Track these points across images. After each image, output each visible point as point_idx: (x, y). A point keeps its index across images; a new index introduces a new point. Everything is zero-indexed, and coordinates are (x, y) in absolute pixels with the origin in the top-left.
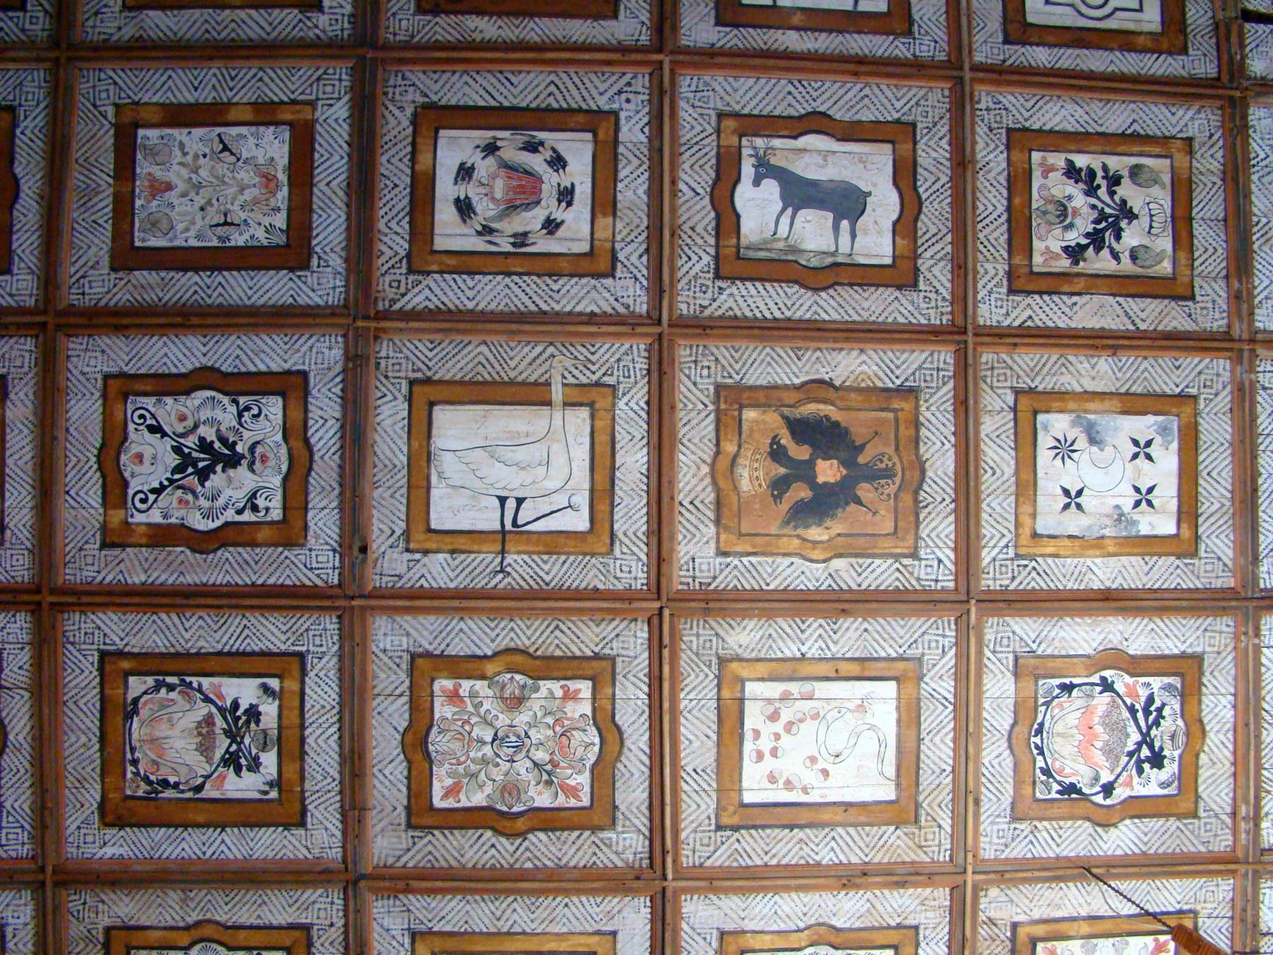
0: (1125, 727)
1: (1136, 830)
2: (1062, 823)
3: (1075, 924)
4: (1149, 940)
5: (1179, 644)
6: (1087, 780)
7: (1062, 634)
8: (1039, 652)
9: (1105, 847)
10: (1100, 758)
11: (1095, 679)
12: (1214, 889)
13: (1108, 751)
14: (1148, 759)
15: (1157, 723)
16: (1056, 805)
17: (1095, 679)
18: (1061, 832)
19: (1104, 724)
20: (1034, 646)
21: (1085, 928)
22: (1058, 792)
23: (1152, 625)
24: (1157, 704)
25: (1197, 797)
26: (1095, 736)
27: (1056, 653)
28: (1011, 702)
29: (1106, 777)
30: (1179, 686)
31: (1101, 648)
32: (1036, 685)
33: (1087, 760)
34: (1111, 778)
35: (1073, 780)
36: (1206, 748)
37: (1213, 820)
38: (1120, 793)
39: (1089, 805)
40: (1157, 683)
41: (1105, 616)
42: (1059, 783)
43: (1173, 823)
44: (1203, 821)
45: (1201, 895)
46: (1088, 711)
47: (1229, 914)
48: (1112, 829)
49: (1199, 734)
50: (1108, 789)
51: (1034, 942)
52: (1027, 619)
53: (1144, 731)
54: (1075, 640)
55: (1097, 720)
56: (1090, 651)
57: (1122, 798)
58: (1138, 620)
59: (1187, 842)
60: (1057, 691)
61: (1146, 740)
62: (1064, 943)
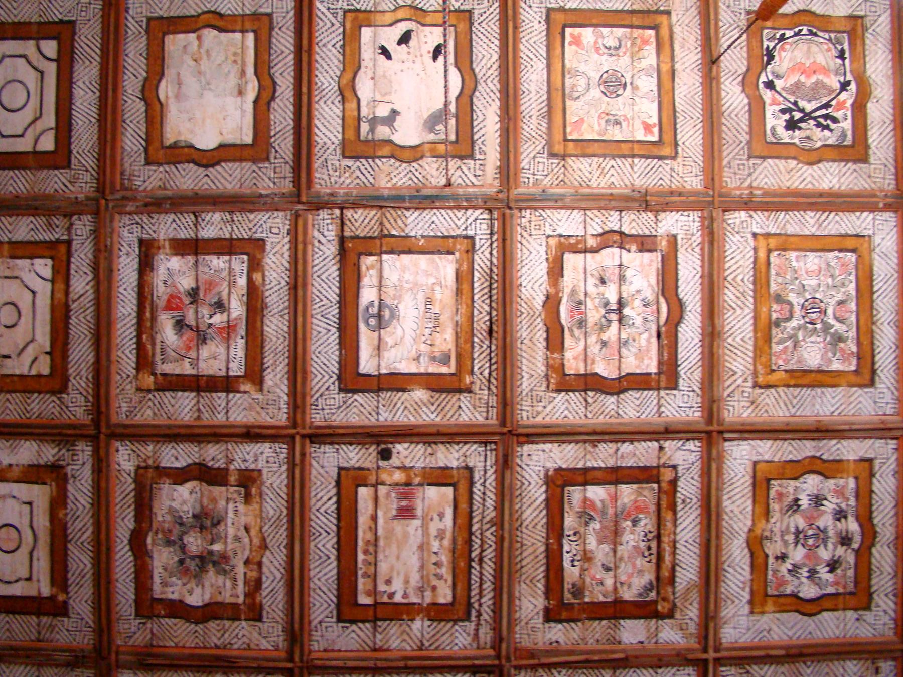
0: (815, 99)
1: (740, 108)
2: (745, 49)
3: (668, 60)
4: (654, 120)
5: (875, 143)
6: (776, 69)
7: (880, 52)
8: (867, 35)
9: (727, 83)
10: (792, 80)
11: (849, 77)
12: (693, 174)
13: (798, 85)
14: (792, 117)
15: (819, 125)
16: (759, 44)
17: (849, 77)
18: (738, 48)
19: (817, 83)
20: (870, 31)
21: (665, 68)
22: (768, 47)
23: (888, 122)
24: (833, 126)
25: (764, 158)
26: (808, 76)
27: (867, 47)
28: (830, 13)
29: (779, 84)
30: (845, 144)
31: (871, 82)
32: (844, 32)
33: (792, 69)
34: (778, 88)
35: (776, 58)
36: (800, 166)
37: (747, 172)
38: (767, 95)
39: (758, 70)
40: (847, 125)
41: (894, 85)
42: (774, 47)
43: (745, 138)
44: (746, 163)
45: (689, 162)
46: (825, 71)
47: (673, 185)
48: (741, 88)
49: (812, 159)
50: (770, 85)
51: (656, 27)
52: (889, 26)
53: (814, 115)
54: (876, 61)
55: (821, 77)
56: (869, 73)
57: (764, 97)
58: (891, 111)
59: (731, 149)
60: (840, 47)
61: (807, 116)
62: (654, 52)
